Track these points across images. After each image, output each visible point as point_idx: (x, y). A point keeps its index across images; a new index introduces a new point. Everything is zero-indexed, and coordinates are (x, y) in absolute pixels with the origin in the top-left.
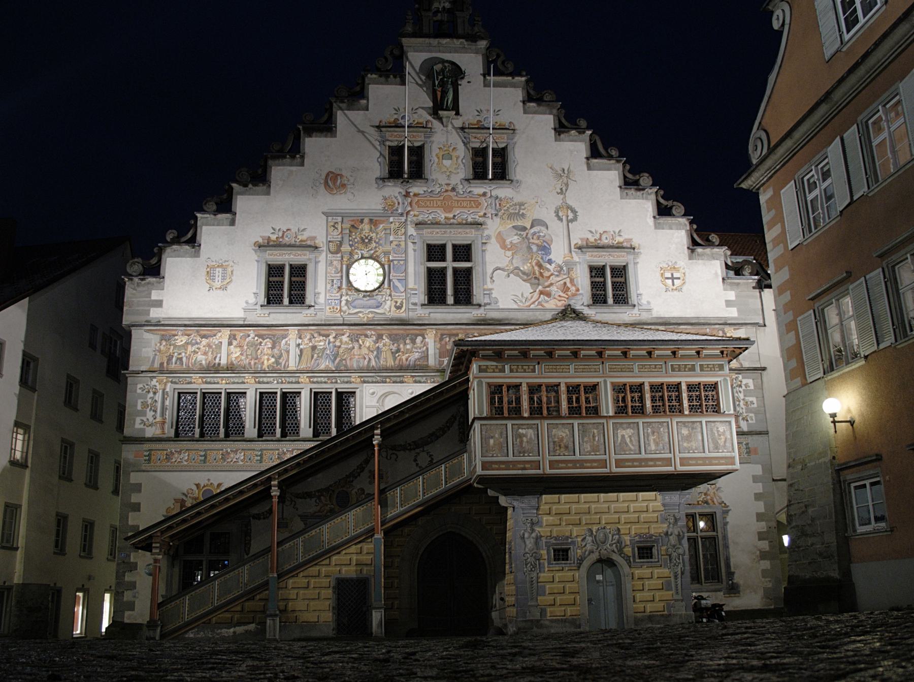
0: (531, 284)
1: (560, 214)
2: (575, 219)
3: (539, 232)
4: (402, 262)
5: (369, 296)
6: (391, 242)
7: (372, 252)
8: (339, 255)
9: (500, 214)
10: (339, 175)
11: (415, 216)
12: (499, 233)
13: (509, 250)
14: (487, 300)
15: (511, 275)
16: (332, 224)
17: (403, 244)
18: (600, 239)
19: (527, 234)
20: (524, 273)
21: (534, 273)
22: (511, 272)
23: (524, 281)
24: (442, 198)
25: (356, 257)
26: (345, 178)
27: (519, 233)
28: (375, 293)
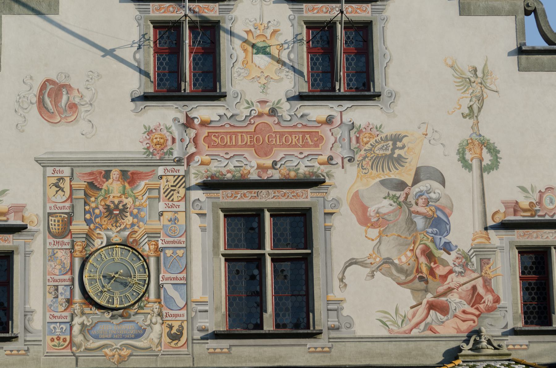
0: (414, 290)
1: (468, 156)
2: (494, 165)
3: (428, 192)
4: (180, 252)
5: (122, 316)
6: (161, 214)
7: (127, 233)
8: (67, 240)
9: (357, 157)
10: (64, 86)
11: (202, 164)
12: (356, 195)
13: (373, 226)
14: (333, 322)
15: (378, 274)
16: (54, 181)
17: (181, 217)
18: (540, 203)
19: (407, 195)
20: (400, 270)
21: (418, 271)
22: (379, 268)
23: (399, 284)
24: (251, 129)
25: (97, 243)
26: (75, 93)
27: (392, 193)
28: (132, 311)
